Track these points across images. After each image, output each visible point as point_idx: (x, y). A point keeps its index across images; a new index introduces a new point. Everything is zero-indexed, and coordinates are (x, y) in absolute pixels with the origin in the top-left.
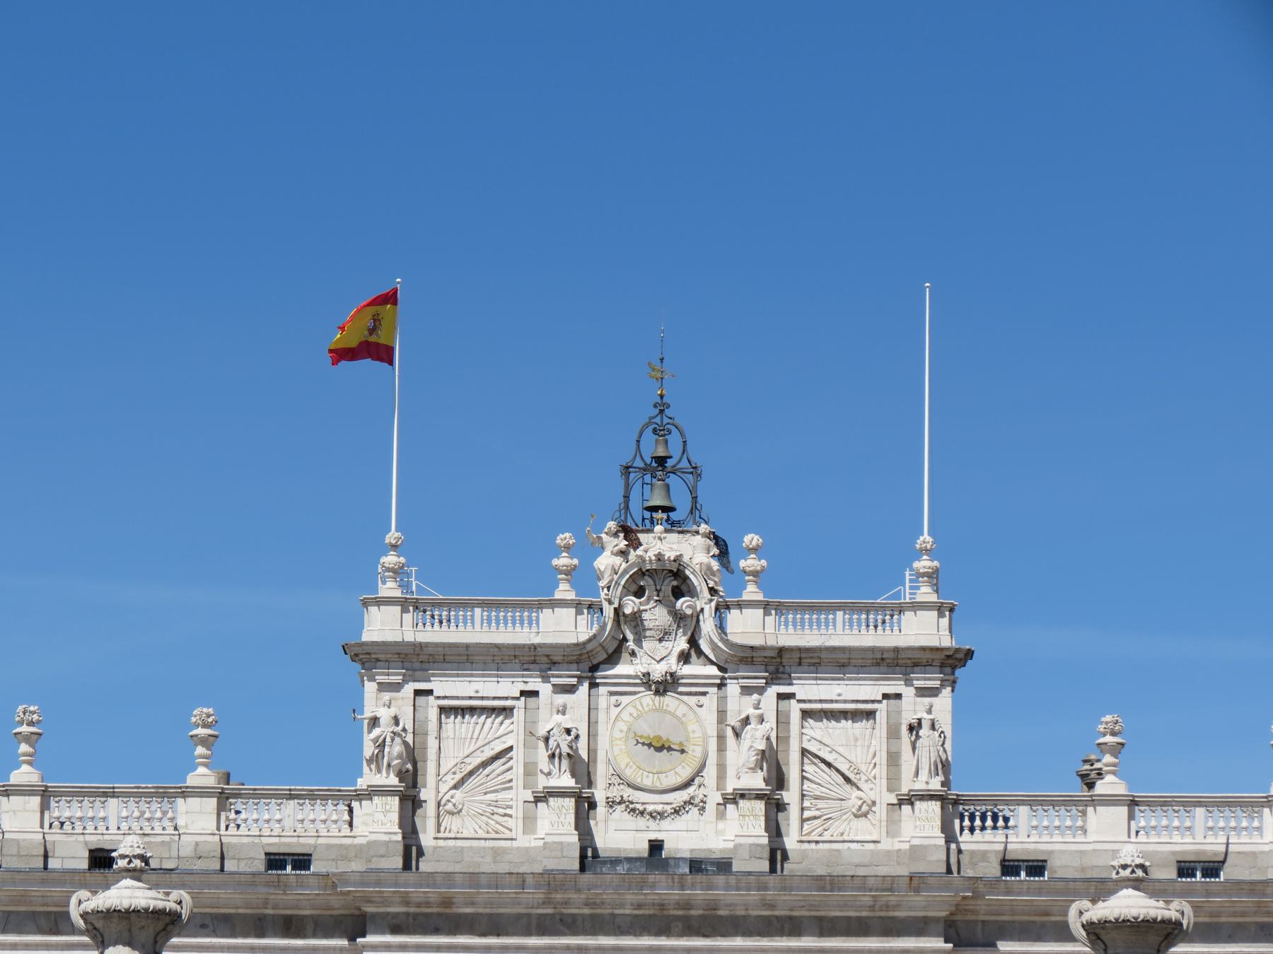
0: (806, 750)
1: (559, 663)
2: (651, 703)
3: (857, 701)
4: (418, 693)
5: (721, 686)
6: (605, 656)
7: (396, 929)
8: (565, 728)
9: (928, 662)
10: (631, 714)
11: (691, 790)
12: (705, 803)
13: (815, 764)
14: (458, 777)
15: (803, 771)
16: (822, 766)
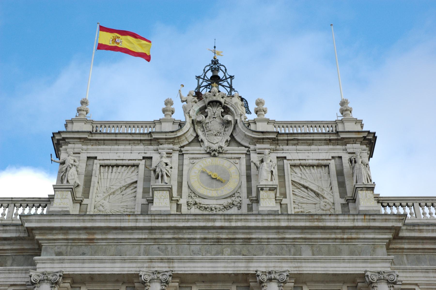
0: (294, 181)
1: (164, 144)
2: (211, 161)
3: (319, 160)
4: (88, 158)
5: (248, 155)
6: (187, 143)
7: (59, 254)
8: (165, 163)
9: (353, 141)
10: (200, 166)
11: (233, 199)
12: (241, 204)
13: (299, 188)
14: (106, 195)
15: (293, 191)
16: (303, 189)
